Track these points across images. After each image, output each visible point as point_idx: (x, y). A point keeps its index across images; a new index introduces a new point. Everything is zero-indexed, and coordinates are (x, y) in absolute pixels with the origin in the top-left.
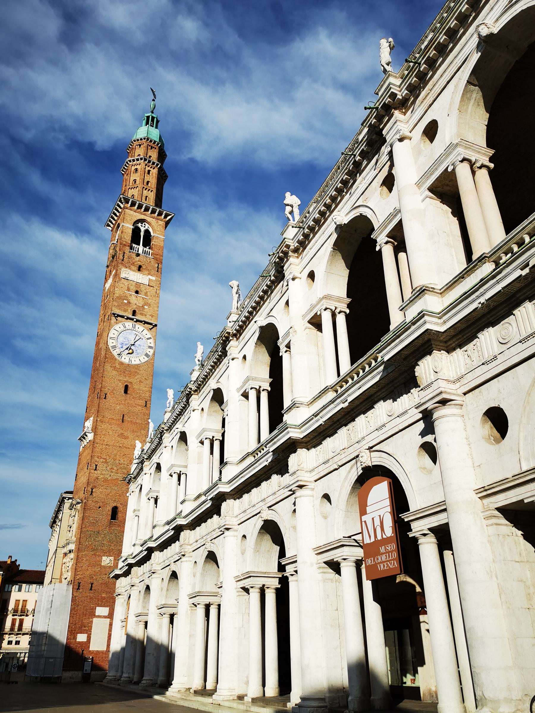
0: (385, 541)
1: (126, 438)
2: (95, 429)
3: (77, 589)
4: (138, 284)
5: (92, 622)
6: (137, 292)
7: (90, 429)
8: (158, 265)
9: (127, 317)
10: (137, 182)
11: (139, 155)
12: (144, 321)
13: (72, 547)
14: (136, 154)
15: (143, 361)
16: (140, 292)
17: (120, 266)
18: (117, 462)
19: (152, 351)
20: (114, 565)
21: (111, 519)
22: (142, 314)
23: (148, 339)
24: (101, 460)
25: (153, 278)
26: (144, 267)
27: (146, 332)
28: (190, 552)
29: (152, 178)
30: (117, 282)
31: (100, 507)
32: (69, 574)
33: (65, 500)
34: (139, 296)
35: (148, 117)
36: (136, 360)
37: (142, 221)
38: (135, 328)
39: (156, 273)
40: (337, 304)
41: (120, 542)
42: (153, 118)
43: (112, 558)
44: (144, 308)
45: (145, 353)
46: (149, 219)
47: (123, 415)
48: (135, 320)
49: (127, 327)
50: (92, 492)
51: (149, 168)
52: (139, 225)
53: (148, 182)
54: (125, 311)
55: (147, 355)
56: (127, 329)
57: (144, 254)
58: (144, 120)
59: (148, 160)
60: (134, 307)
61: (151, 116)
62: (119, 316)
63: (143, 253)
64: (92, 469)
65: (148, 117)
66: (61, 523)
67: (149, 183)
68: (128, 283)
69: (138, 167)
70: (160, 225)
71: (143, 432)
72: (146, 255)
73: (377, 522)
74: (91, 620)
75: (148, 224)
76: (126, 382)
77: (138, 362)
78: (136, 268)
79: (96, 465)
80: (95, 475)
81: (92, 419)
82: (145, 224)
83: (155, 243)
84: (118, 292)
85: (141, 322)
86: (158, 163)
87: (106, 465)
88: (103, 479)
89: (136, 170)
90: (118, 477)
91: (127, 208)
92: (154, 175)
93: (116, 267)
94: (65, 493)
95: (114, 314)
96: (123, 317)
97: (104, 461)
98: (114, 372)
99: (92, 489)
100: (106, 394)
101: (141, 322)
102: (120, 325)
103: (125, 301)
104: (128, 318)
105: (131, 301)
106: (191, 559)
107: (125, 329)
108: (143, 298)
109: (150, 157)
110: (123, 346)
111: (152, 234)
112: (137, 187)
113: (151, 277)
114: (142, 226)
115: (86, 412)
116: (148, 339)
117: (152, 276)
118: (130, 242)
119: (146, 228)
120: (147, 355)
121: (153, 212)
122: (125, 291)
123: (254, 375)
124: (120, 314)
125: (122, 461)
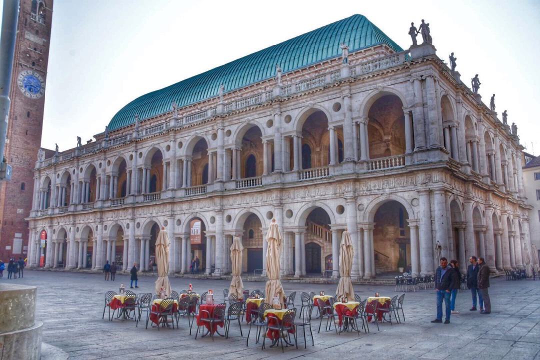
0: (198, 236)
5: (13, 241)
6: (35, 49)
18: (24, 158)
24: (15, 156)
25: (45, 41)
26: (40, 32)
43: (22, 210)
47: (27, 131)
62: (24, 65)
73: (196, 230)
77: (35, 97)
95: (21, 64)
101: (38, 70)
103: (28, 55)
113: (44, 40)
116: (42, 82)
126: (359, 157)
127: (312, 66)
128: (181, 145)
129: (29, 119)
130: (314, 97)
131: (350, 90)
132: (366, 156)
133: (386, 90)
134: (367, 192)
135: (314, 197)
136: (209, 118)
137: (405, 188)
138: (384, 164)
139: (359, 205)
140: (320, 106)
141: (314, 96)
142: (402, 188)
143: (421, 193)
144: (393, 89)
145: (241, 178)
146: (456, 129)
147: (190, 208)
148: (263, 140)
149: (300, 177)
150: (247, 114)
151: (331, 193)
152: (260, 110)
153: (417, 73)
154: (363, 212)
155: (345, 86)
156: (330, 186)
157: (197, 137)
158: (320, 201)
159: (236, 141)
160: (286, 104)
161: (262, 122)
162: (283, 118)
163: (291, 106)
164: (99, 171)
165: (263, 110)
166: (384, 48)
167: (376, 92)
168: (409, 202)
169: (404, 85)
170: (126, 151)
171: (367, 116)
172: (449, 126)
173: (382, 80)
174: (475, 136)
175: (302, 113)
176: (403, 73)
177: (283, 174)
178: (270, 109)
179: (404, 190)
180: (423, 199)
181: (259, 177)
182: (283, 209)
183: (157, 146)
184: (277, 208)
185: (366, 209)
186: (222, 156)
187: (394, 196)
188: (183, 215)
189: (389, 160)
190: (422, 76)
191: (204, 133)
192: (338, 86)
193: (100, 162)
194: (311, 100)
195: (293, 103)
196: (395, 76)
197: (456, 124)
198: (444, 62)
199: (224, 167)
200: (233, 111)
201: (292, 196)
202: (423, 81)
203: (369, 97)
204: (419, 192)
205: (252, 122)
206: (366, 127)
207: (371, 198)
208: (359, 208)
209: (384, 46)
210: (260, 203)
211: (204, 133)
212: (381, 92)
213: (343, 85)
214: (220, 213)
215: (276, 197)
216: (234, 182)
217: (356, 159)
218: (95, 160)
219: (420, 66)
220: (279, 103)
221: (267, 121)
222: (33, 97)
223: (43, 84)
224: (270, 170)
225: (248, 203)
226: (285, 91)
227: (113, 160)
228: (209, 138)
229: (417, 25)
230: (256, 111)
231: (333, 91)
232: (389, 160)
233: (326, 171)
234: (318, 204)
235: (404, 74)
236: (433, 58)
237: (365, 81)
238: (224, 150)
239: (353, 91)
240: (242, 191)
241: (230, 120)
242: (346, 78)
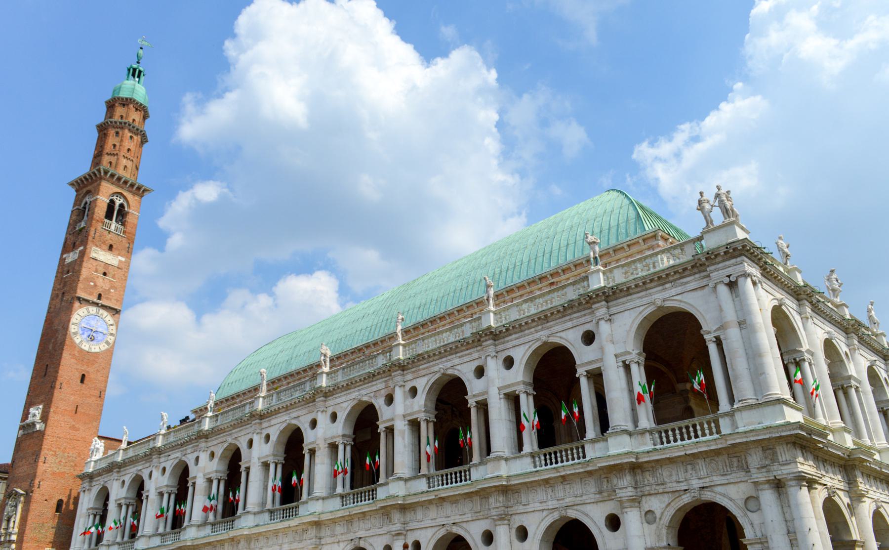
1: (77, 430)
6: (105, 274)
7: (38, 417)
15: (103, 349)
16: (108, 274)
17: (90, 244)
18: (66, 454)
22: (107, 299)
23: (110, 325)
25: (123, 259)
26: (114, 246)
31: (46, 500)
36: (95, 348)
37: (117, 194)
38: (98, 313)
39: (127, 253)
44: (110, 292)
46: (125, 193)
48: (100, 305)
49: (91, 312)
52: (115, 198)
54: (91, 294)
55: (107, 343)
60: (100, 291)
61: (138, 70)
71: (95, 424)
76: (83, 370)
77: (97, 350)
79: (45, 458)
80: (44, 468)
84: (84, 273)
87: (55, 458)
91: (105, 179)
95: (79, 299)
96: (87, 301)
98: (73, 361)
99: (39, 482)
100: (61, 384)
105: (98, 284)
113: (120, 258)
116: (110, 325)
117: (122, 256)
119: (122, 201)
120: (107, 343)
125: (71, 454)
126: (635, 421)
127: (543, 275)
128: (334, 417)
129: (84, 385)
130: (549, 324)
131: (608, 308)
132: (648, 420)
133: (668, 304)
134: (657, 488)
135: (563, 499)
136: (380, 368)
137: (728, 477)
138: (681, 434)
139: (647, 513)
140: (561, 338)
141: (548, 322)
142: (723, 478)
143: (761, 487)
144: (681, 301)
145: (436, 470)
146: (810, 364)
147: (349, 531)
148: (470, 401)
149: (534, 462)
150: (441, 358)
151: (593, 490)
152: (462, 351)
153: (720, 272)
154: (654, 526)
155: (598, 302)
156: (590, 479)
157: (360, 402)
158: (575, 507)
159: (425, 406)
160: (504, 337)
161: (466, 373)
162: (500, 362)
163: (512, 341)
164: (193, 471)
165: (467, 350)
166: (660, 238)
167: (651, 309)
168: (741, 503)
169: (699, 293)
170: (243, 433)
171: (642, 351)
172: (795, 359)
173: (660, 288)
174: (850, 377)
175: (530, 351)
176: (695, 273)
177: (506, 459)
178: (479, 348)
179: (726, 482)
180: (768, 497)
181: (466, 467)
182: (509, 525)
183: (294, 422)
184: (499, 522)
185: (660, 519)
186: (403, 432)
187: (709, 493)
188: (336, 545)
189: (690, 425)
190: (729, 276)
191: (372, 395)
192: (587, 303)
193: (195, 455)
194: (543, 329)
195: (514, 336)
196: (682, 281)
197: (807, 356)
198: (766, 251)
199: (406, 453)
200: (419, 355)
201: (524, 500)
202: (732, 285)
203: (641, 318)
204: (756, 484)
205: (450, 372)
206: (642, 368)
207: (666, 499)
208: (649, 516)
209: (660, 234)
210: (470, 515)
211: (372, 395)
212: (660, 308)
213: (595, 300)
214: (400, 537)
215: (497, 501)
216: (424, 479)
217: (630, 427)
218: (189, 451)
219: (724, 261)
220: (491, 336)
221: (474, 368)
222: (93, 351)
223: (113, 327)
224: (485, 452)
225: (448, 517)
226: (501, 318)
227: (219, 451)
228: (379, 403)
229: (710, 196)
230: (457, 353)
231: (579, 311)
232: (690, 425)
233: (580, 450)
234: (573, 514)
235: (697, 276)
236: (744, 246)
237: (631, 291)
238: (407, 422)
239: (614, 310)
240: (437, 493)
241: (413, 370)
242: (598, 290)
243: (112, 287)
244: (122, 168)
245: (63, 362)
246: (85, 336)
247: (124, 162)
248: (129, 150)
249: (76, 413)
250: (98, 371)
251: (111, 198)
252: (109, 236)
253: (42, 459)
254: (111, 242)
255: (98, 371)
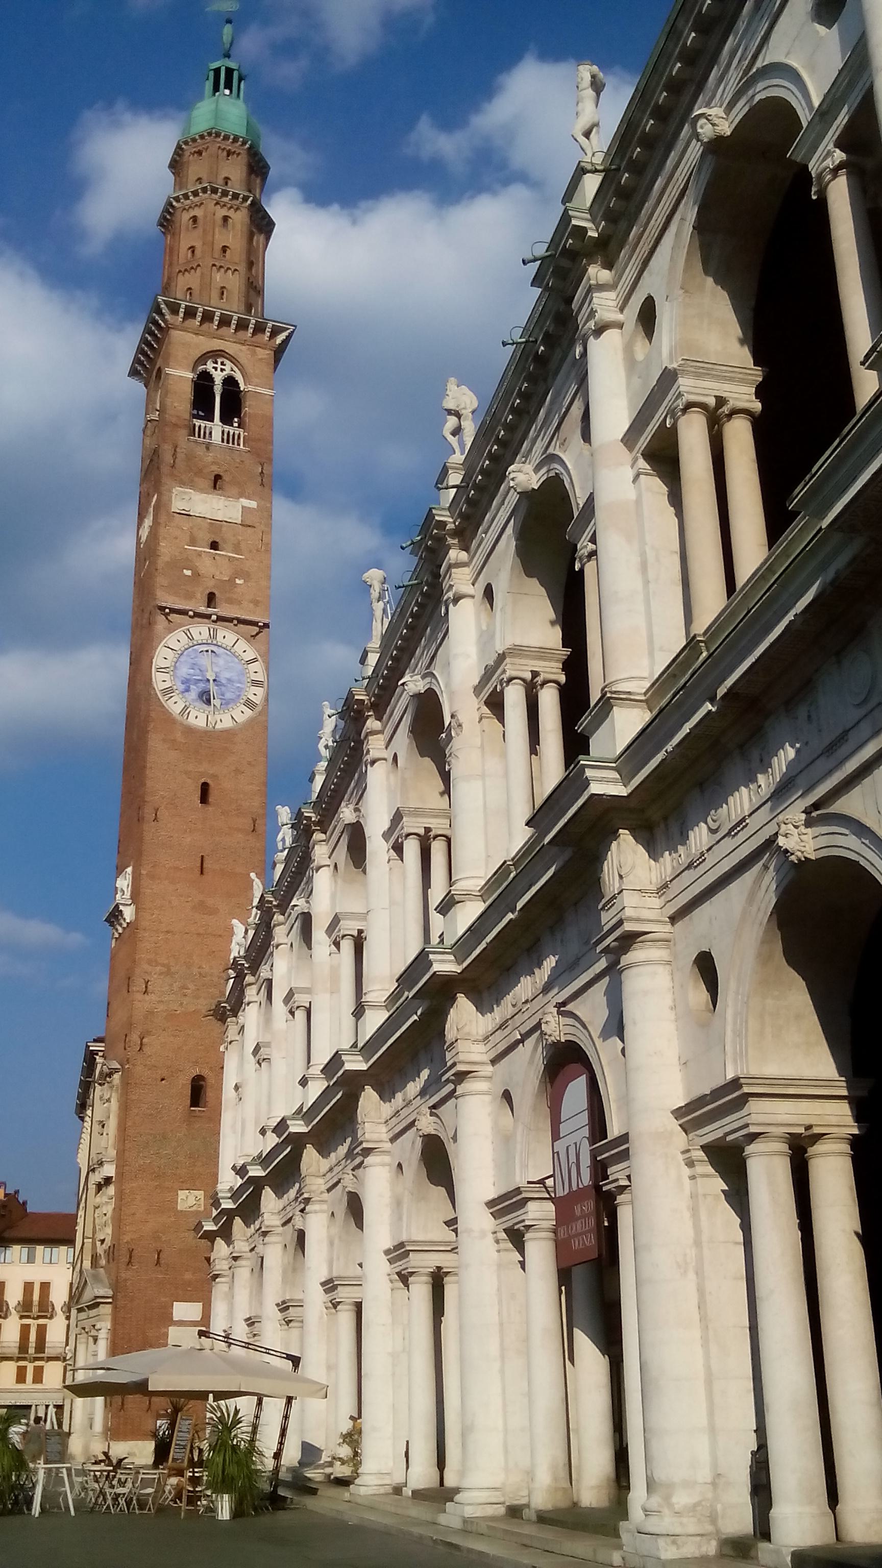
1: (213, 912)
2: (136, 897)
3: (128, 1264)
4: (216, 524)
6: (214, 546)
8: (262, 469)
9: (194, 612)
10: (198, 252)
11: (199, 180)
12: (237, 619)
13: (109, 1170)
14: (192, 177)
15: (241, 718)
18: (195, 970)
19: (260, 691)
20: (205, 1209)
21: (191, 1106)
22: (230, 601)
24: (158, 968)
25: (253, 504)
26: (226, 477)
27: (242, 645)
28: (322, 1193)
29: (234, 236)
30: (164, 525)
31: (163, 1080)
32: (109, 1230)
33: (97, 1057)
34: (219, 554)
35: (217, 71)
37: (215, 355)
38: (215, 637)
39: (260, 488)
40: (538, 665)
41: (213, 1158)
42: (229, 72)
43: (200, 1194)
45: (245, 698)
46: (231, 348)
47: (202, 857)
48: (214, 617)
50: (141, 1044)
51: (224, 212)
52: (210, 366)
53: (224, 249)
54: (189, 596)
55: (249, 704)
56: (195, 643)
57: (225, 444)
58: (208, 79)
59: (220, 190)
62: (173, 611)
63: (223, 441)
64: (138, 991)
65: (217, 71)
66: (93, 1110)
67: (228, 251)
68: (191, 525)
69: (197, 212)
70: (262, 359)
72: (230, 445)
74: (164, 1330)
75: (232, 362)
78: (210, 483)
81: (129, 870)
82: (222, 364)
83: (251, 411)
84: (166, 550)
85: (230, 620)
86: (246, 194)
88: (165, 1014)
89: (195, 219)
90: (199, 1007)
92: (238, 227)
93: (157, 486)
94: (95, 1041)
95: (162, 609)
97: (164, 969)
101: (230, 620)
102: (179, 634)
103: (188, 573)
104: (197, 615)
105: (202, 571)
106: (325, 1207)
107: (191, 644)
108: (230, 557)
109: (227, 179)
110: (189, 687)
111: (242, 387)
112: (199, 265)
113: (245, 502)
114: (216, 369)
115: (119, 852)
117: (249, 498)
118: (187, 416)
120: (249, 704)
121: (242, 325)
122: (186, 547)
123: (413, 804)
124: (176, 607)
243: (237, 574)
244: (215, 294)
245: (151, 759)
246: (193, 694)
247: (218, 278)
248: (224, 249)
249: (202, 873)
250: (237, 771)
251: (201, 368)
252: (209, 457)
253: (138, 985)
254: (216, 469)
255: (237, 771)
